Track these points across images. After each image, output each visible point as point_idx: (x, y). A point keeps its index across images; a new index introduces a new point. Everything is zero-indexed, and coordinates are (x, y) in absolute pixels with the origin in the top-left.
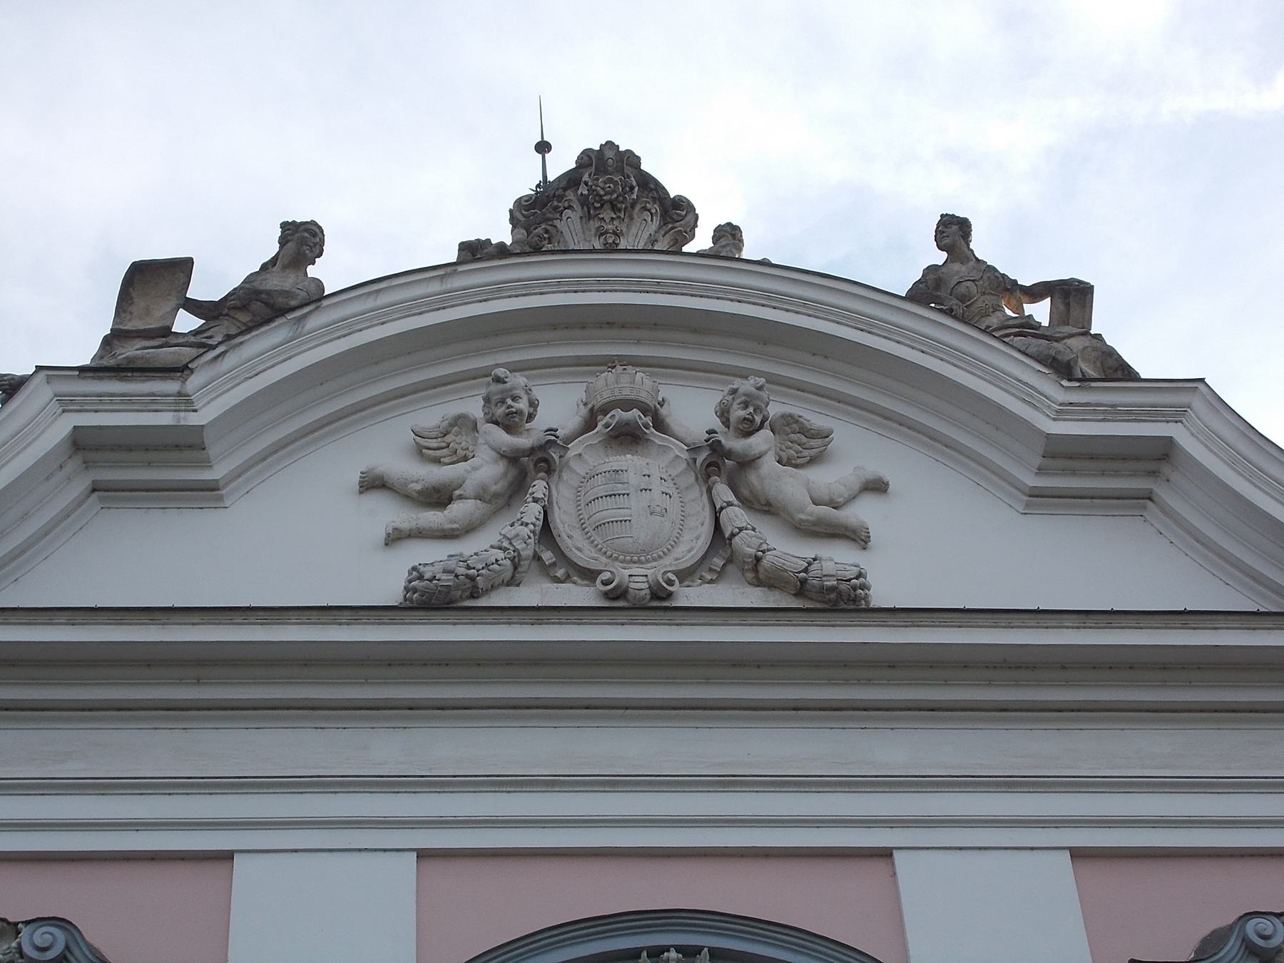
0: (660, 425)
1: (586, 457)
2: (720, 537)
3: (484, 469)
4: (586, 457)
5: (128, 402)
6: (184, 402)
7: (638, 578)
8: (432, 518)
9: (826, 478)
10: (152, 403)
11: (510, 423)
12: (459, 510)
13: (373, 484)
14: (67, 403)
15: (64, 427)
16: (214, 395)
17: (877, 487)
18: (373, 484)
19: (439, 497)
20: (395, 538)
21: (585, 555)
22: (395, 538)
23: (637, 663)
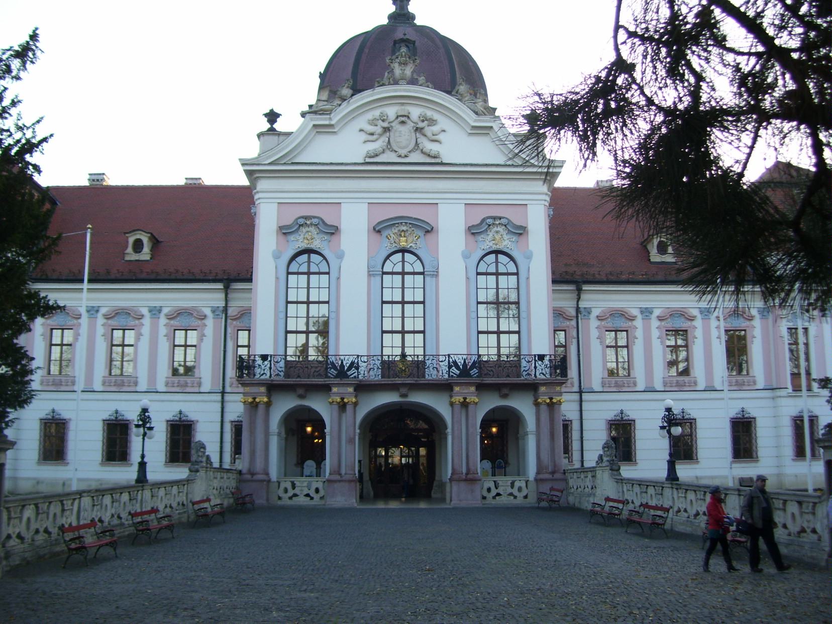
0: (408, 117)
1: (396, 125)
2: (417, 144)
3: (379, 130)
4: (396, 125)
5: (321, 119)
6: (330, 119)
7: (403, 152)
8: (371, 138)
9: (435, 129)
10: (325, 119)
11: (383, 121)
12: (375, 137)
13: (361, 130)
14: (312, 120)
15: (311, 125)
16: (335, 118)
17: (444, 131)
18: (361, 130)
19: (372, 134)
20: (365, 142)
21: (395, 148)
22: (365, 142)
23: (402, 170)
